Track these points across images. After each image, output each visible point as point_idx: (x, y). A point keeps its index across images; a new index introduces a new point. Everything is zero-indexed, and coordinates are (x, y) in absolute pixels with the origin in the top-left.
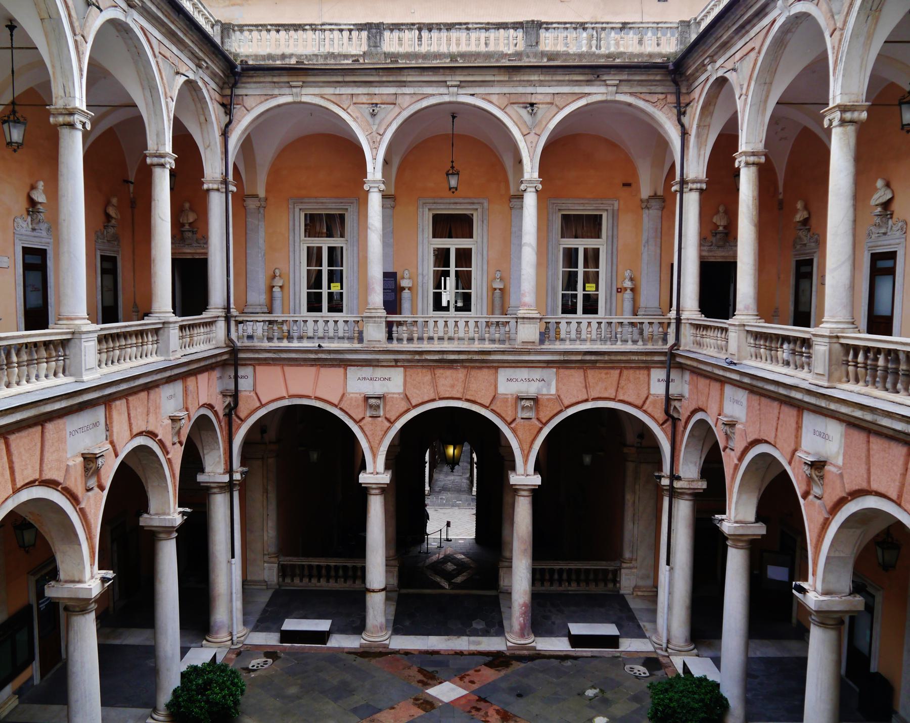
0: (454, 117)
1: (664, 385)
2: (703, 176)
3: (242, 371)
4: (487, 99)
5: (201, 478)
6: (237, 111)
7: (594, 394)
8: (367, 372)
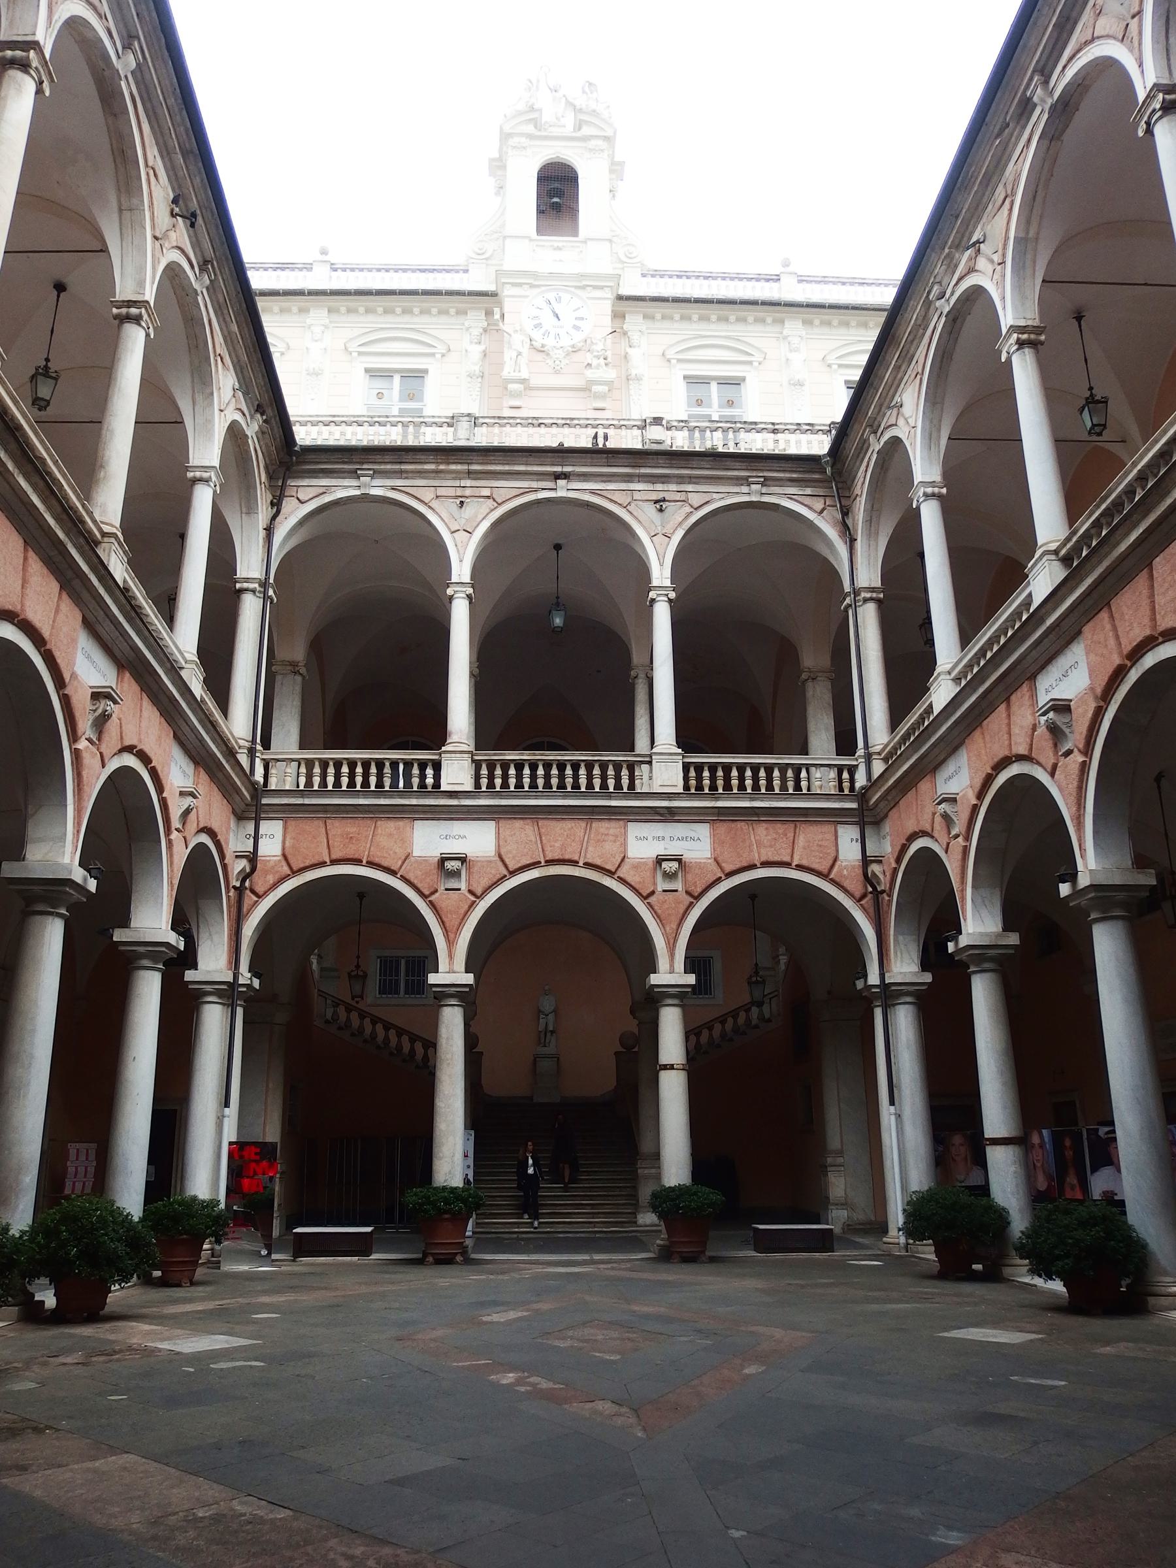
1: (857, 846)
2: (879, 584)
3: (265, 827)
5: (190, 975)
6: (288, 505)
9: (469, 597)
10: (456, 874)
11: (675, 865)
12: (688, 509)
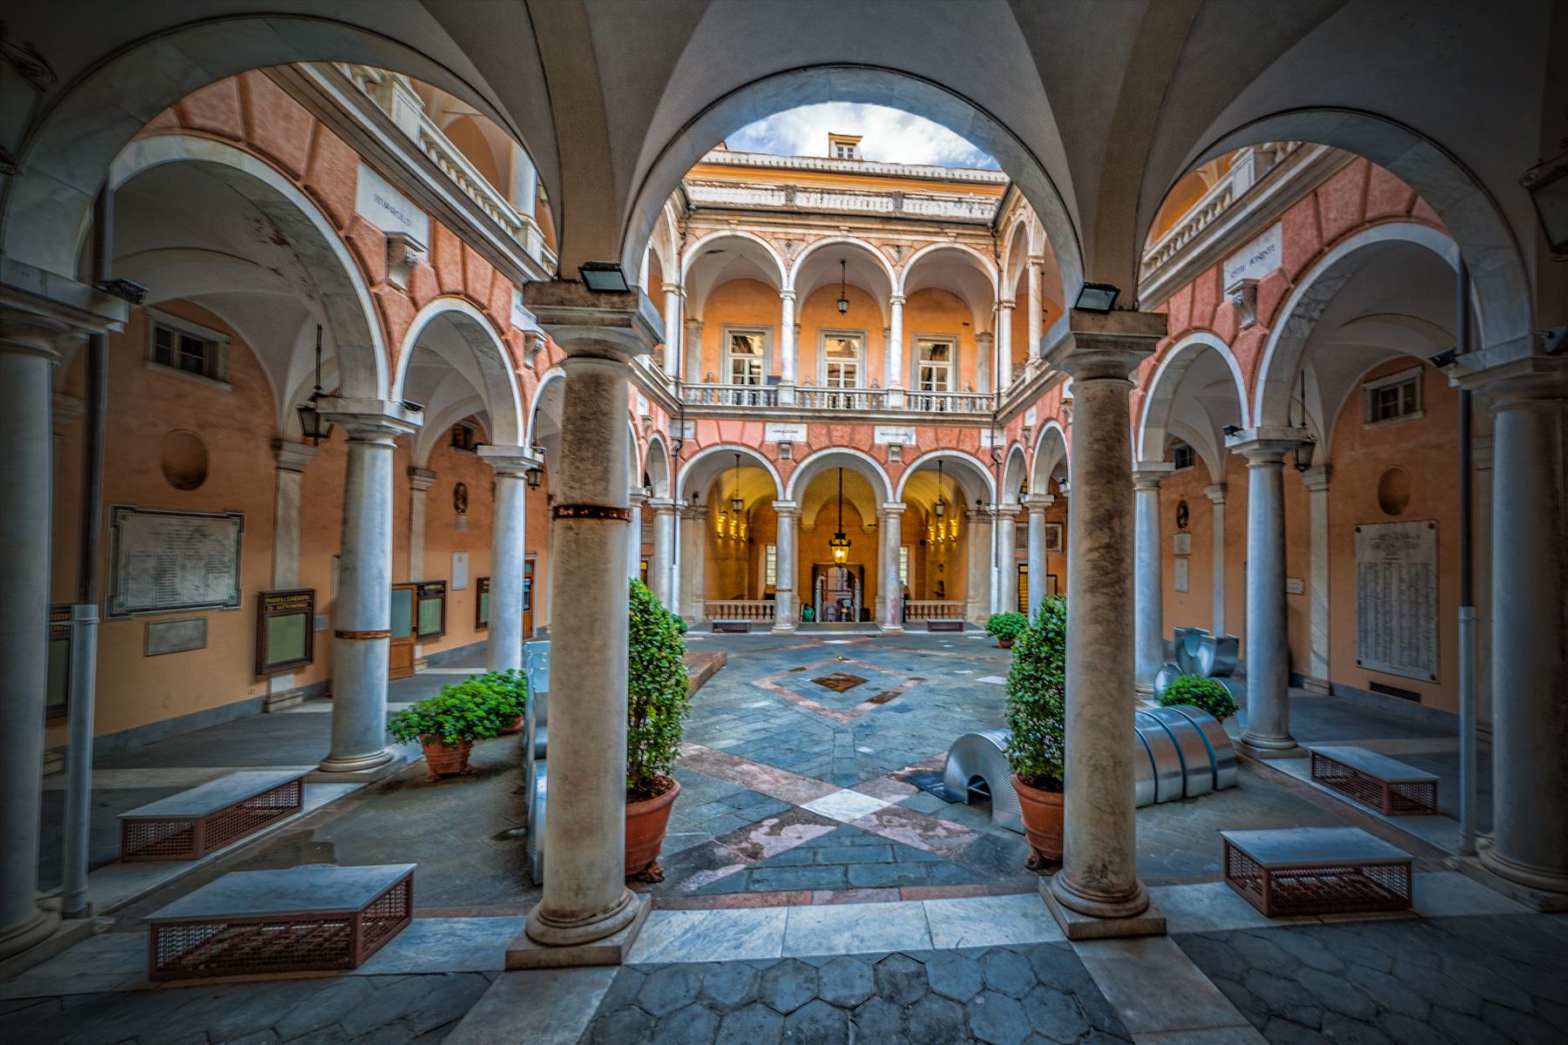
4: (868, 241)
7: (942, 445)
8: (780, 426)
10: (786, 451)
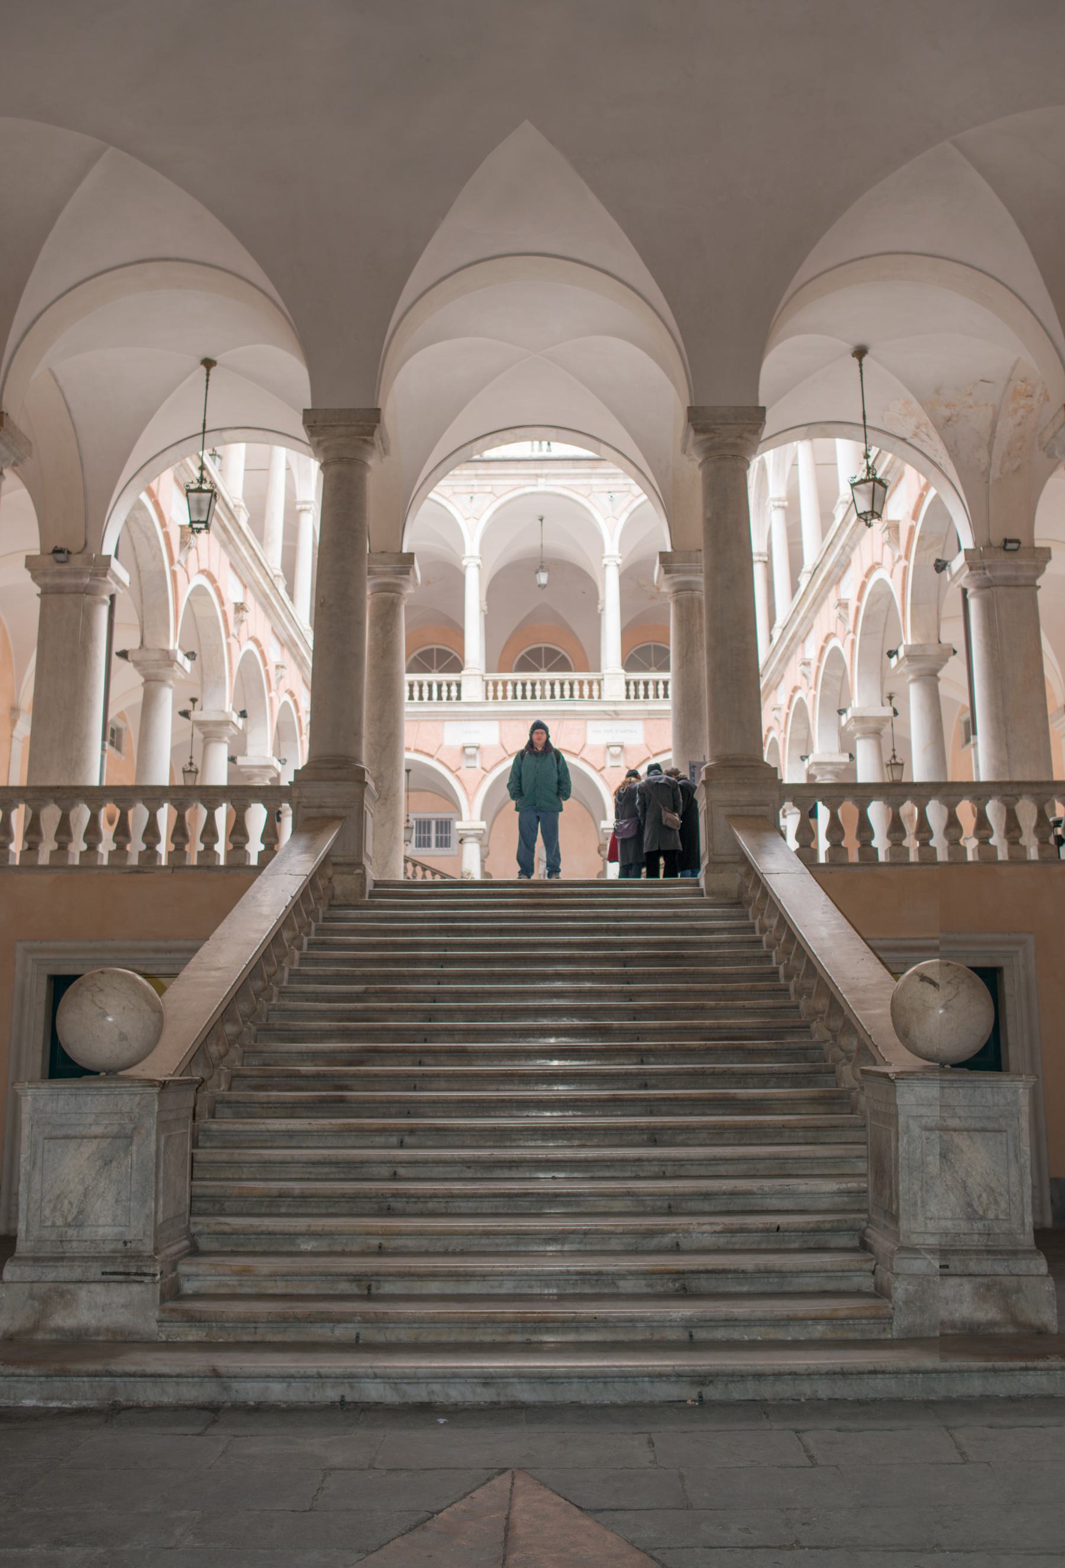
0: (541, 520)
9: (478, 566)
10: (472, 757)
11: (616, 750)
12: (630, 497)
